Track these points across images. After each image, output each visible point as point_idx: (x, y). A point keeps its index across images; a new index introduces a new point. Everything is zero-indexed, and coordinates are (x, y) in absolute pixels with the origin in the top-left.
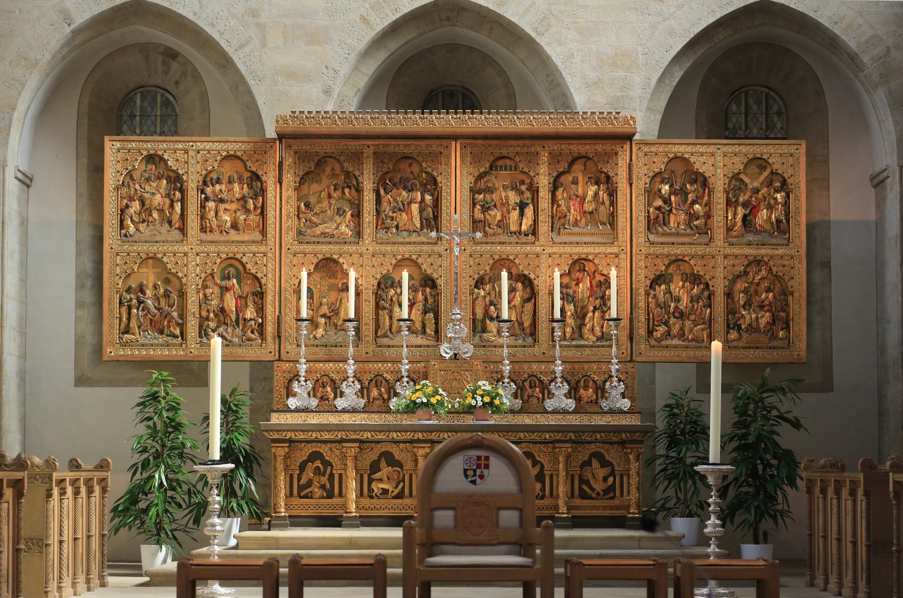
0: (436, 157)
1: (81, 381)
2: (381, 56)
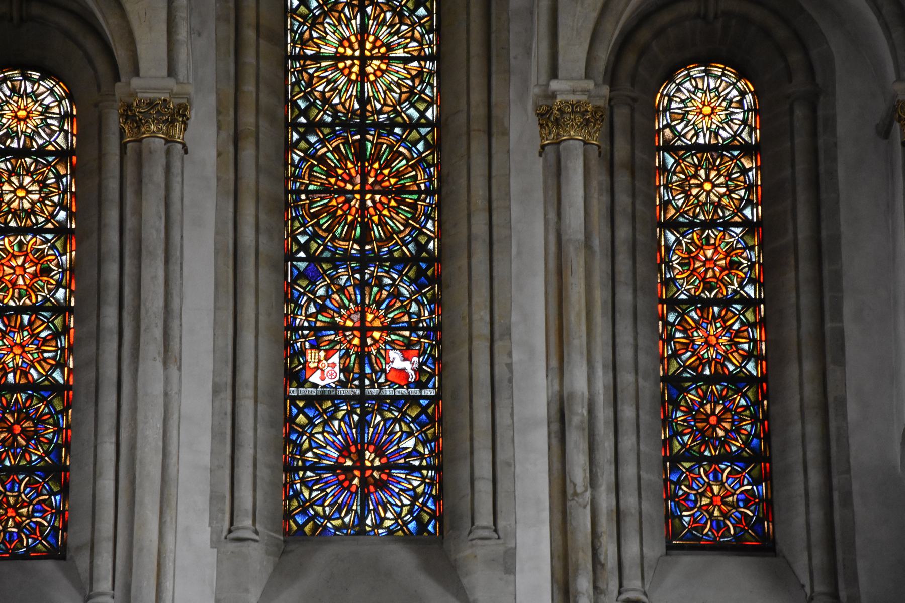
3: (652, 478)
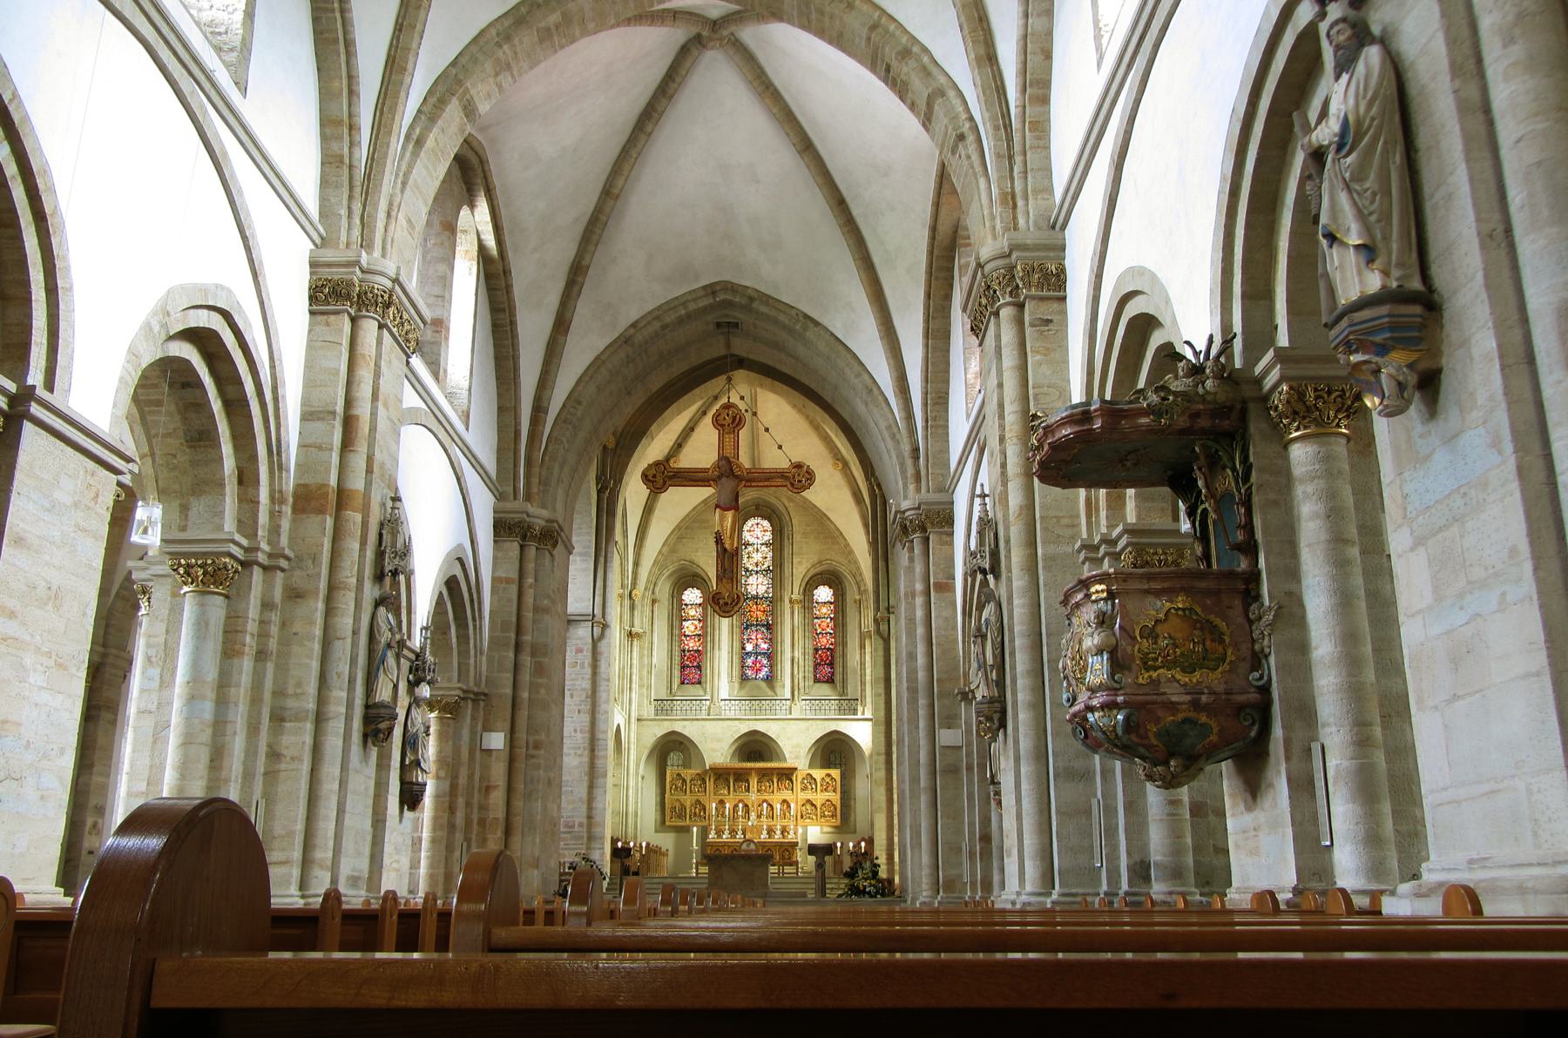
0: (750, 774)
1: (656, 831)
2: (736, 744)
3: (811, 669)
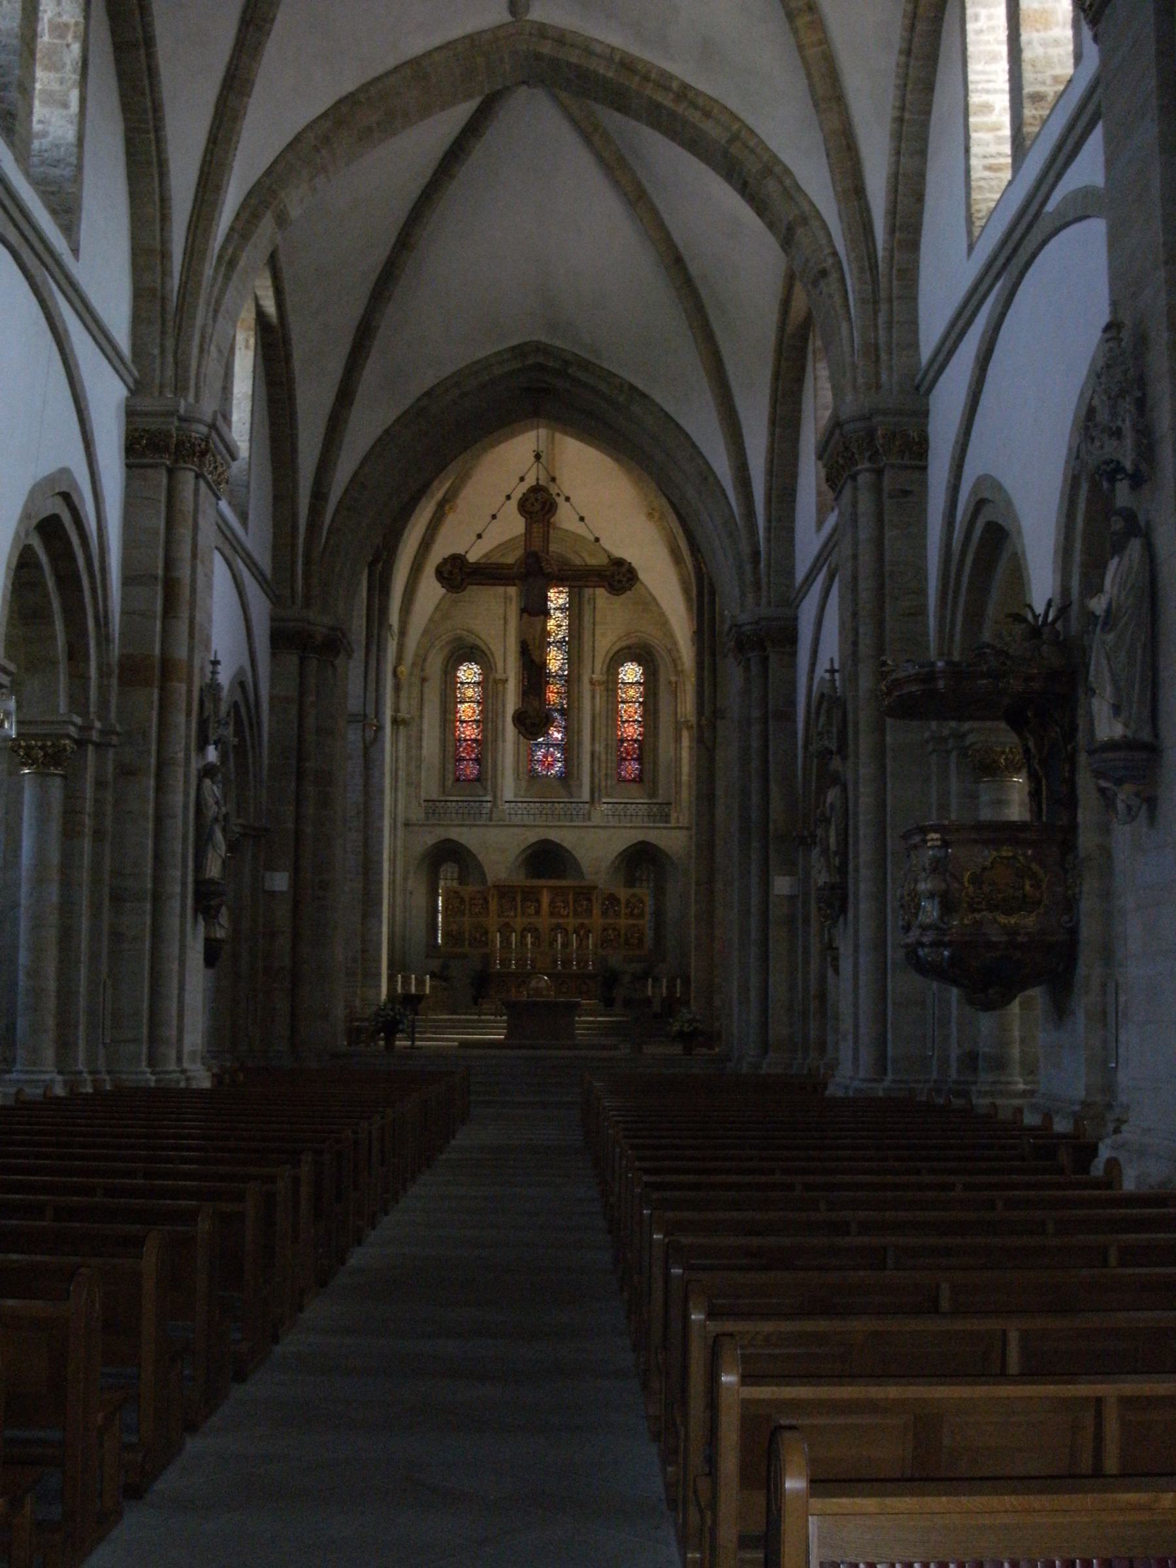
1: (428, 956)
